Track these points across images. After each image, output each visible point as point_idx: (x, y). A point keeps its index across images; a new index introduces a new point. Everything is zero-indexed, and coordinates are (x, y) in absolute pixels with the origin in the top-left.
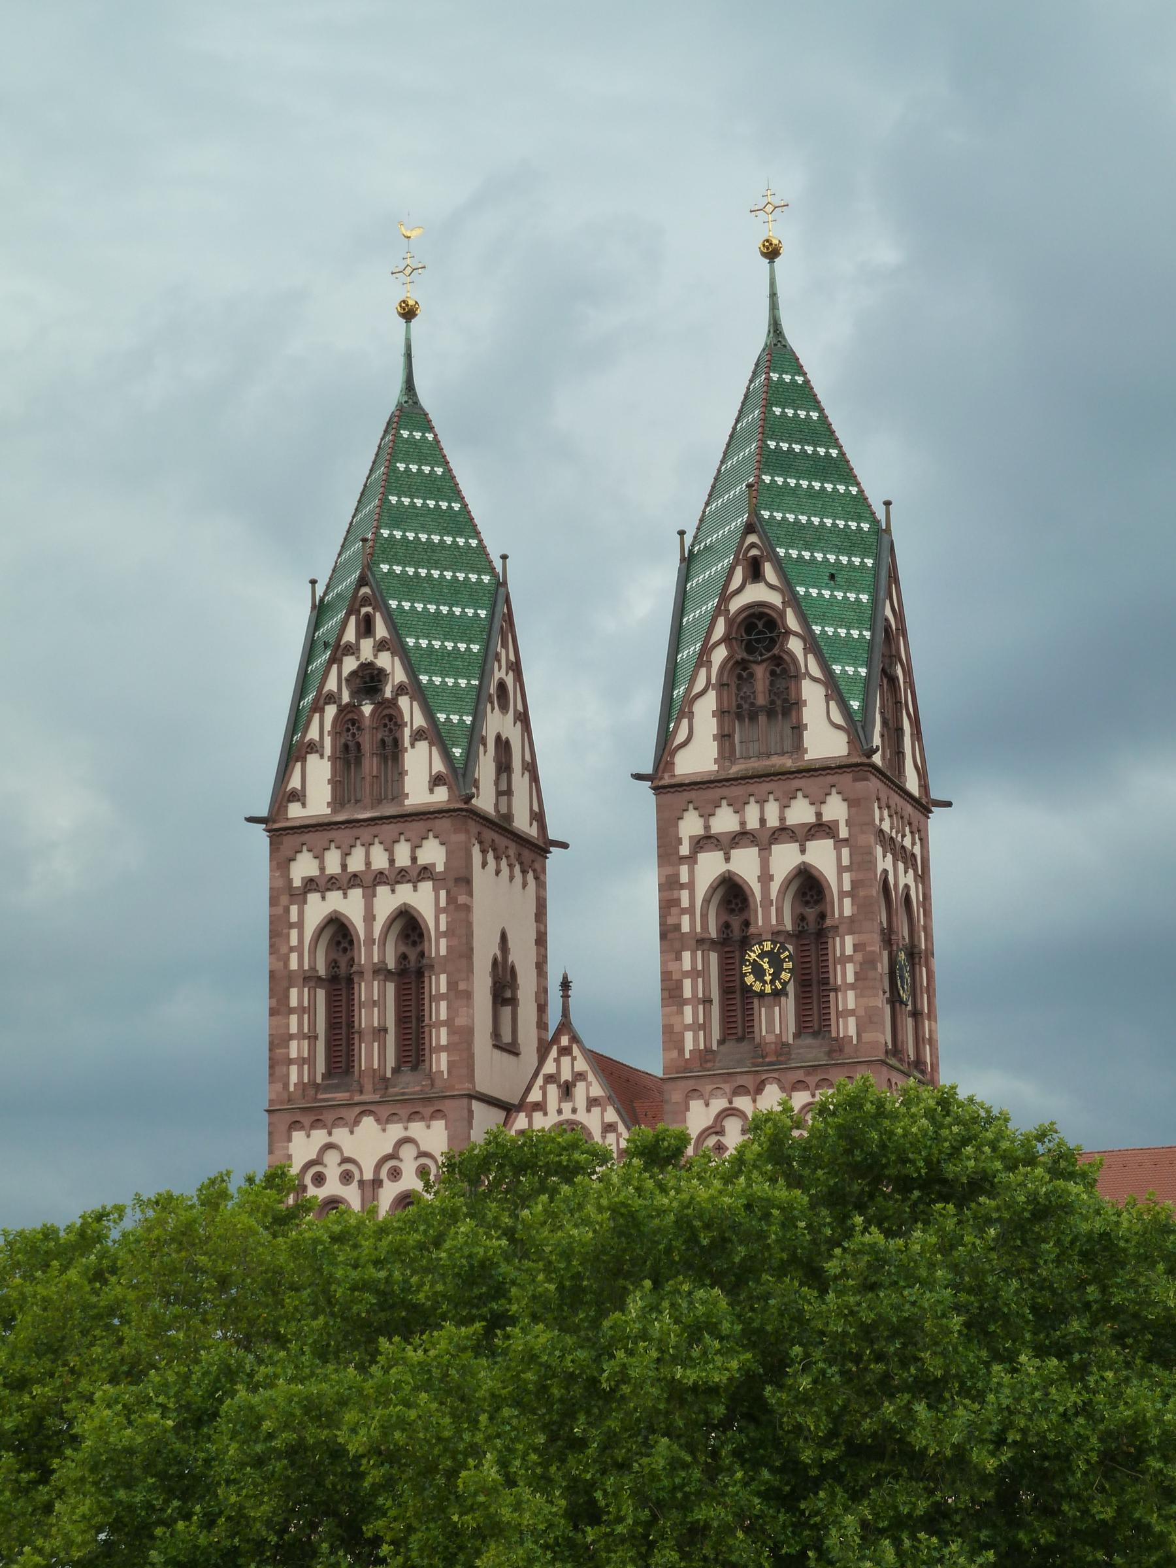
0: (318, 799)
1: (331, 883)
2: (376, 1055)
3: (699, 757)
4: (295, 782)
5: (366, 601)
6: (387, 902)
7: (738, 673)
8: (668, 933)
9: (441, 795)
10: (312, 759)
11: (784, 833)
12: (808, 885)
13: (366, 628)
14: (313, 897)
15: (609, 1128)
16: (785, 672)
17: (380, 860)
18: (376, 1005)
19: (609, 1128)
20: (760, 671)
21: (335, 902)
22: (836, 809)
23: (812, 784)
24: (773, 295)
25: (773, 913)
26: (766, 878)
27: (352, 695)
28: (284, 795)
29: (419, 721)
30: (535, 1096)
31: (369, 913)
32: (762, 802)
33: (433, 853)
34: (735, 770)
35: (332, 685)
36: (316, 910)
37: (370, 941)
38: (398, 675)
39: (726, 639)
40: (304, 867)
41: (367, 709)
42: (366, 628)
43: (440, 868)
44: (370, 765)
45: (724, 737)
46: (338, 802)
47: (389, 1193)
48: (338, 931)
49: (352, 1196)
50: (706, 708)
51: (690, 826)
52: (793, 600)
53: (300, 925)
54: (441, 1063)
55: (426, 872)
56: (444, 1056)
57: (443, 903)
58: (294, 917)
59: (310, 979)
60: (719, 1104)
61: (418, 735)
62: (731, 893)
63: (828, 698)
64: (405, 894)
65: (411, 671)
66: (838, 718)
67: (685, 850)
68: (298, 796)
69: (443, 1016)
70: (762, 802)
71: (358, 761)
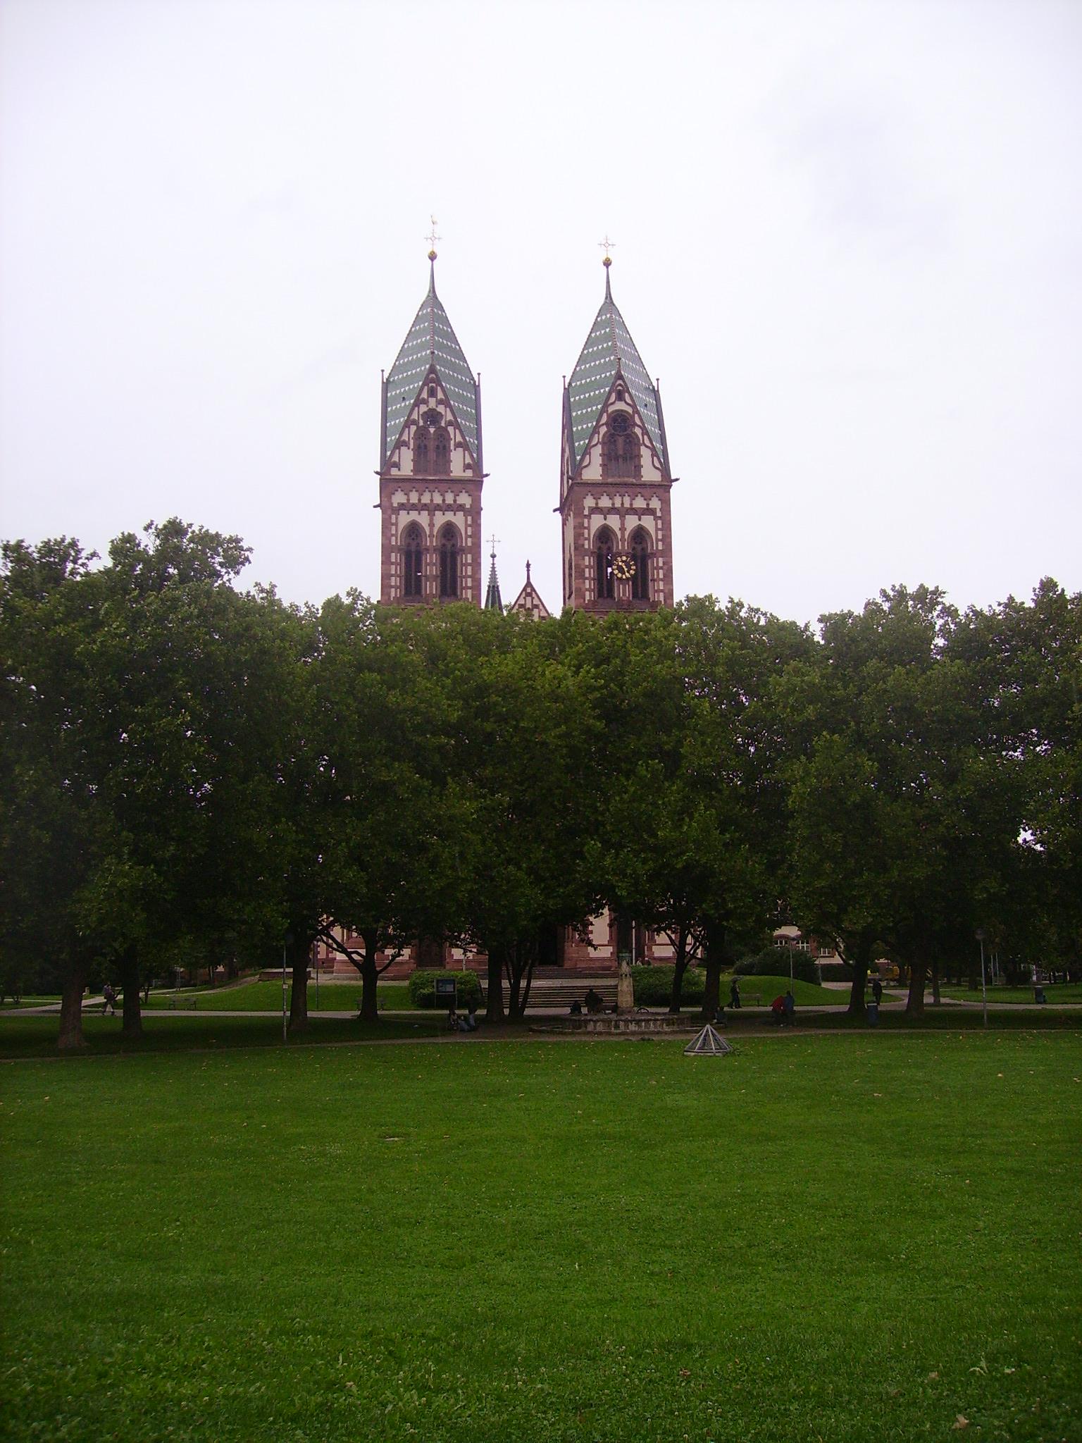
0: (407, 467)
1: (413, 507)
3: (593, 472)
4: (395, 459)
5: (432, 381)
6: (440, 519)
9: (469, 473)
11: (633, 511)
12: (640, 535)
13: (432, 393)
14: (403, 513)
17: (438, 499)
18: (431, 566)
20: (620, 440)
21: (414, 515)
23: (647, 492)
24: (608, 282)
26: (623, 529)
27: (425, 422)
28: (387, 463)
29: (459, 438)
31: (431, 524)
32: (622, 496)
33: (465, 499)
34: (610, 480)
35: (415, 416)
36: (404, 519)
37: (431, 536)
38: (450, 417)
39: (606, 424)
40: (399, 498)
41: (432, 430)
42: (432, 393)
43: (468, 506)
44: (432, 455)
45: (604, 465)
46: (416, 470)
48: (414, 530)
50: (597, 451)
51: (589, 502)
52: (638, 412)
53: (396, 524)
55: (461, 508)
56: (469, 592)
57: (469, 522)
58: (393, 521)
59: (399, 550)
61: (458, 445)
62: (605, 534)
63: (653, 456)
64: (449, 516)
66: (657, 465)
67: (586, 512)
68: (397, 465)
69: (469, 573)
70: (622, 496)
71: (425, 453)
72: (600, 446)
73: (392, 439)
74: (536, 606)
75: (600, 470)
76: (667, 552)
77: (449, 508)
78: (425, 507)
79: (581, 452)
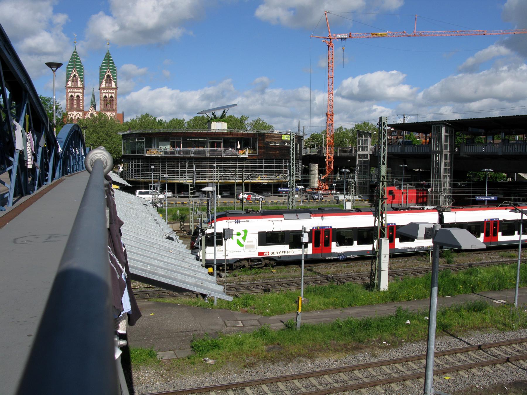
2: (75, 106)
6: (76, 94)
7: (107, 79)
8: (101, 99)
12: (112, 97)
16: (110, 80)
18: (75, 102)
21: (72, 94)
22: (114, 91)
25: (109, 99)
33: (81, 91)
38: (77, 75)
40: (69, 90)
47: (76, 118)
48: (72, 96)
49: (73, 117)
50: (104, 82)
51: (103, 91)
54: (81, 108)
62: (105, 97)
64: (78, 94)
76: (116, 100)
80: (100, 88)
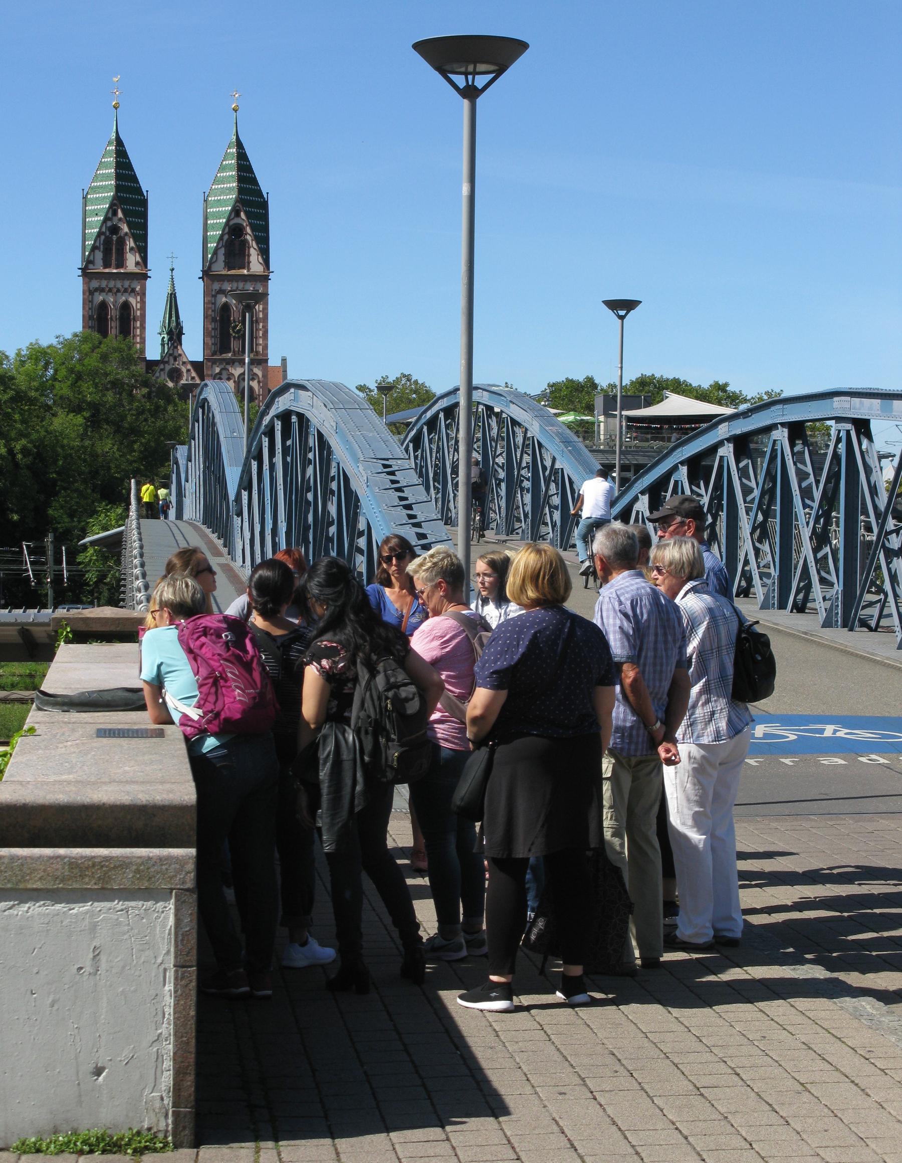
10: (97, 252)
13: (115, 213)
15: (188, 371)
16: (244, 245)
19: (188, 371)
29: (132, 244)
30: (166, 359)
38: (125, 229)
39: (228, 233)
40: (95, 284)
50: (222, 251)
53: (91, 302)
60: (222, 366)
65: (130, 228)
72: (223, 249)
73: (90, 243)
74: (180, 355)
75: (223, 264)
77: (126, 291)
78: (110, 290)
79: (212, 251)
80: (207, 274)
